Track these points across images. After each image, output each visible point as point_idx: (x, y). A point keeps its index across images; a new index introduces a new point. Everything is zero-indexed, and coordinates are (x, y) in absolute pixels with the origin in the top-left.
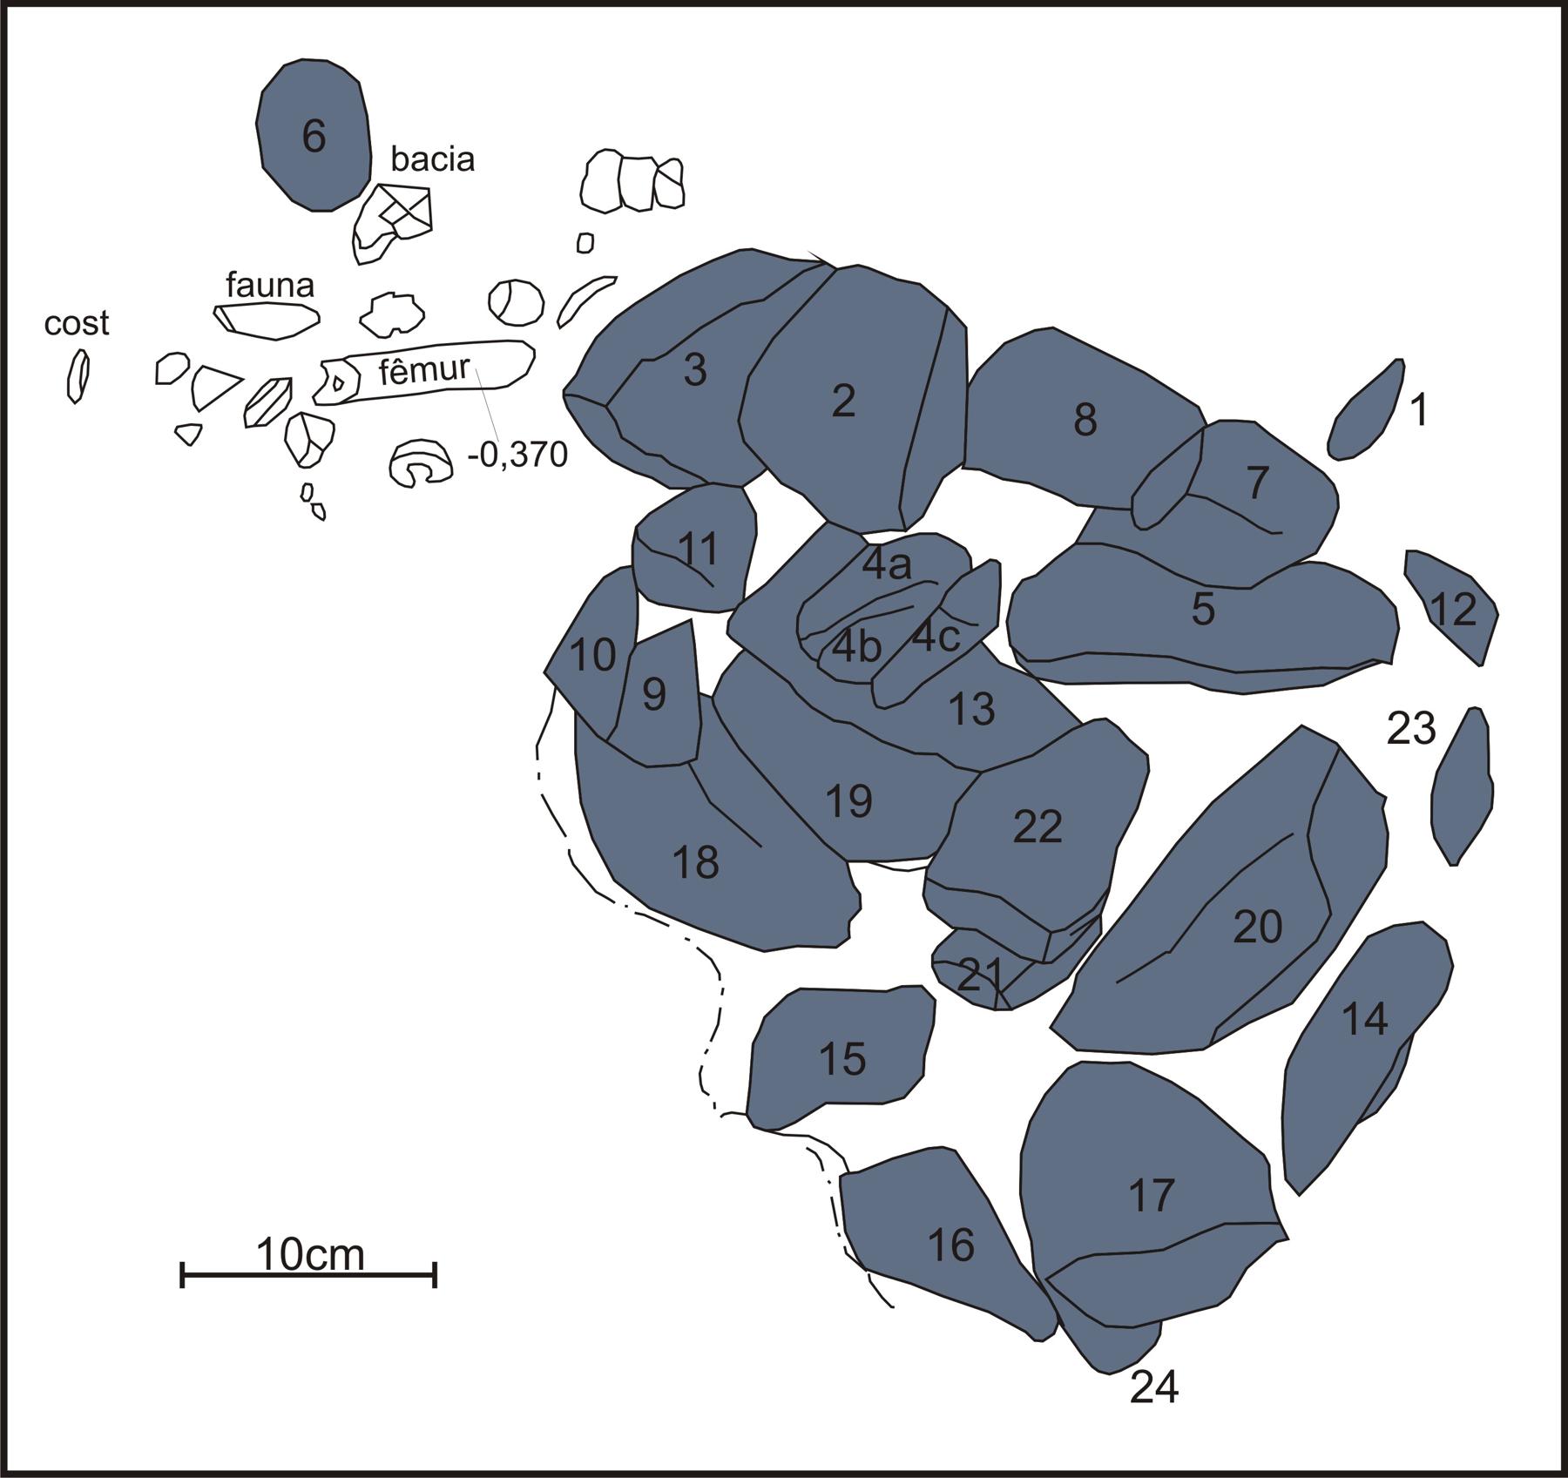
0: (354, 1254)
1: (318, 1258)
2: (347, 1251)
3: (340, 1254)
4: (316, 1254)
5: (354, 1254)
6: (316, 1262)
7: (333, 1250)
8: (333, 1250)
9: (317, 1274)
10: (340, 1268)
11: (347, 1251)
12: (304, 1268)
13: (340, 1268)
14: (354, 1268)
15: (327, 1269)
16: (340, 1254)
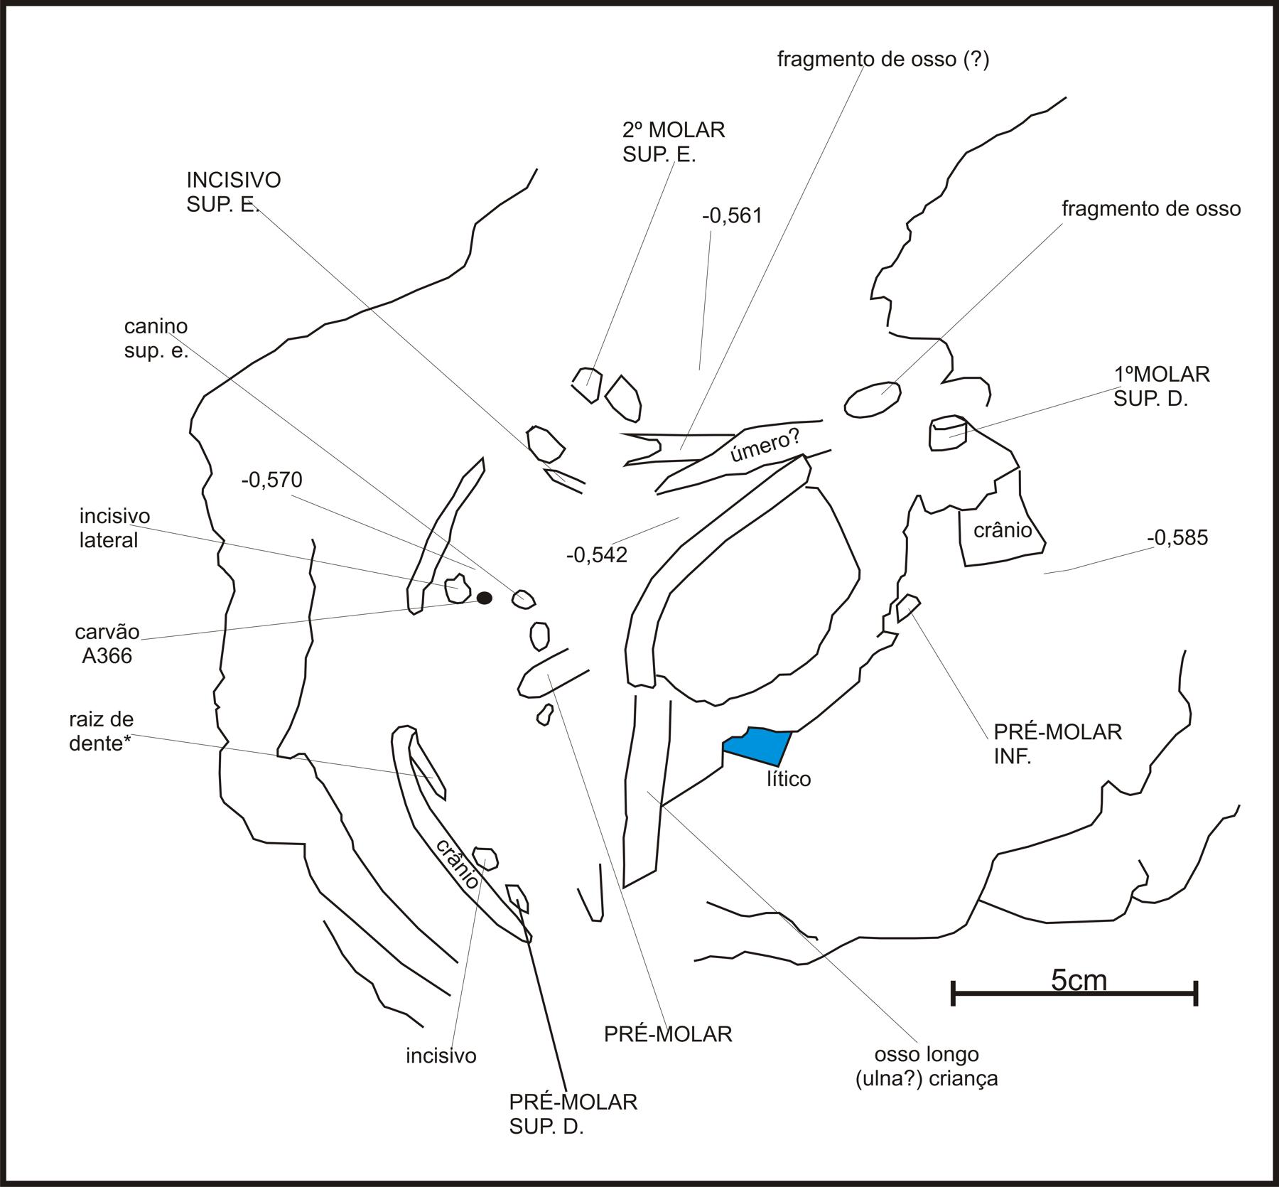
0: (1100, 980)
1: (1076, 983)
2: (1096, 978)
3: (1091, 980)
4: (1075, 979)
5: (1100, 980)
6: (1075, 985)
7: (1086, 977)
8: (1086, 977)
9: (1076, 993)
10: (1091, 988)
11: (1096, 978)
12: (1067, 989)
13: (1091, 988)
14: (1100, 988)
15: (1083, 989)
16: (1091, 980)
